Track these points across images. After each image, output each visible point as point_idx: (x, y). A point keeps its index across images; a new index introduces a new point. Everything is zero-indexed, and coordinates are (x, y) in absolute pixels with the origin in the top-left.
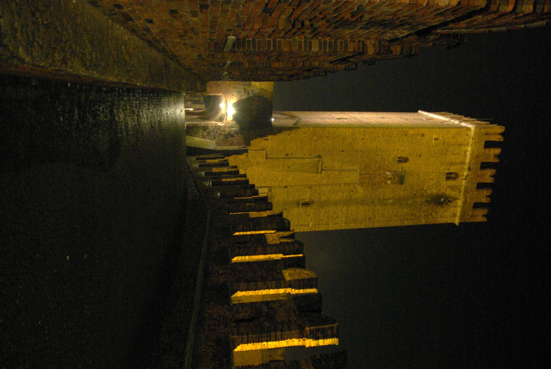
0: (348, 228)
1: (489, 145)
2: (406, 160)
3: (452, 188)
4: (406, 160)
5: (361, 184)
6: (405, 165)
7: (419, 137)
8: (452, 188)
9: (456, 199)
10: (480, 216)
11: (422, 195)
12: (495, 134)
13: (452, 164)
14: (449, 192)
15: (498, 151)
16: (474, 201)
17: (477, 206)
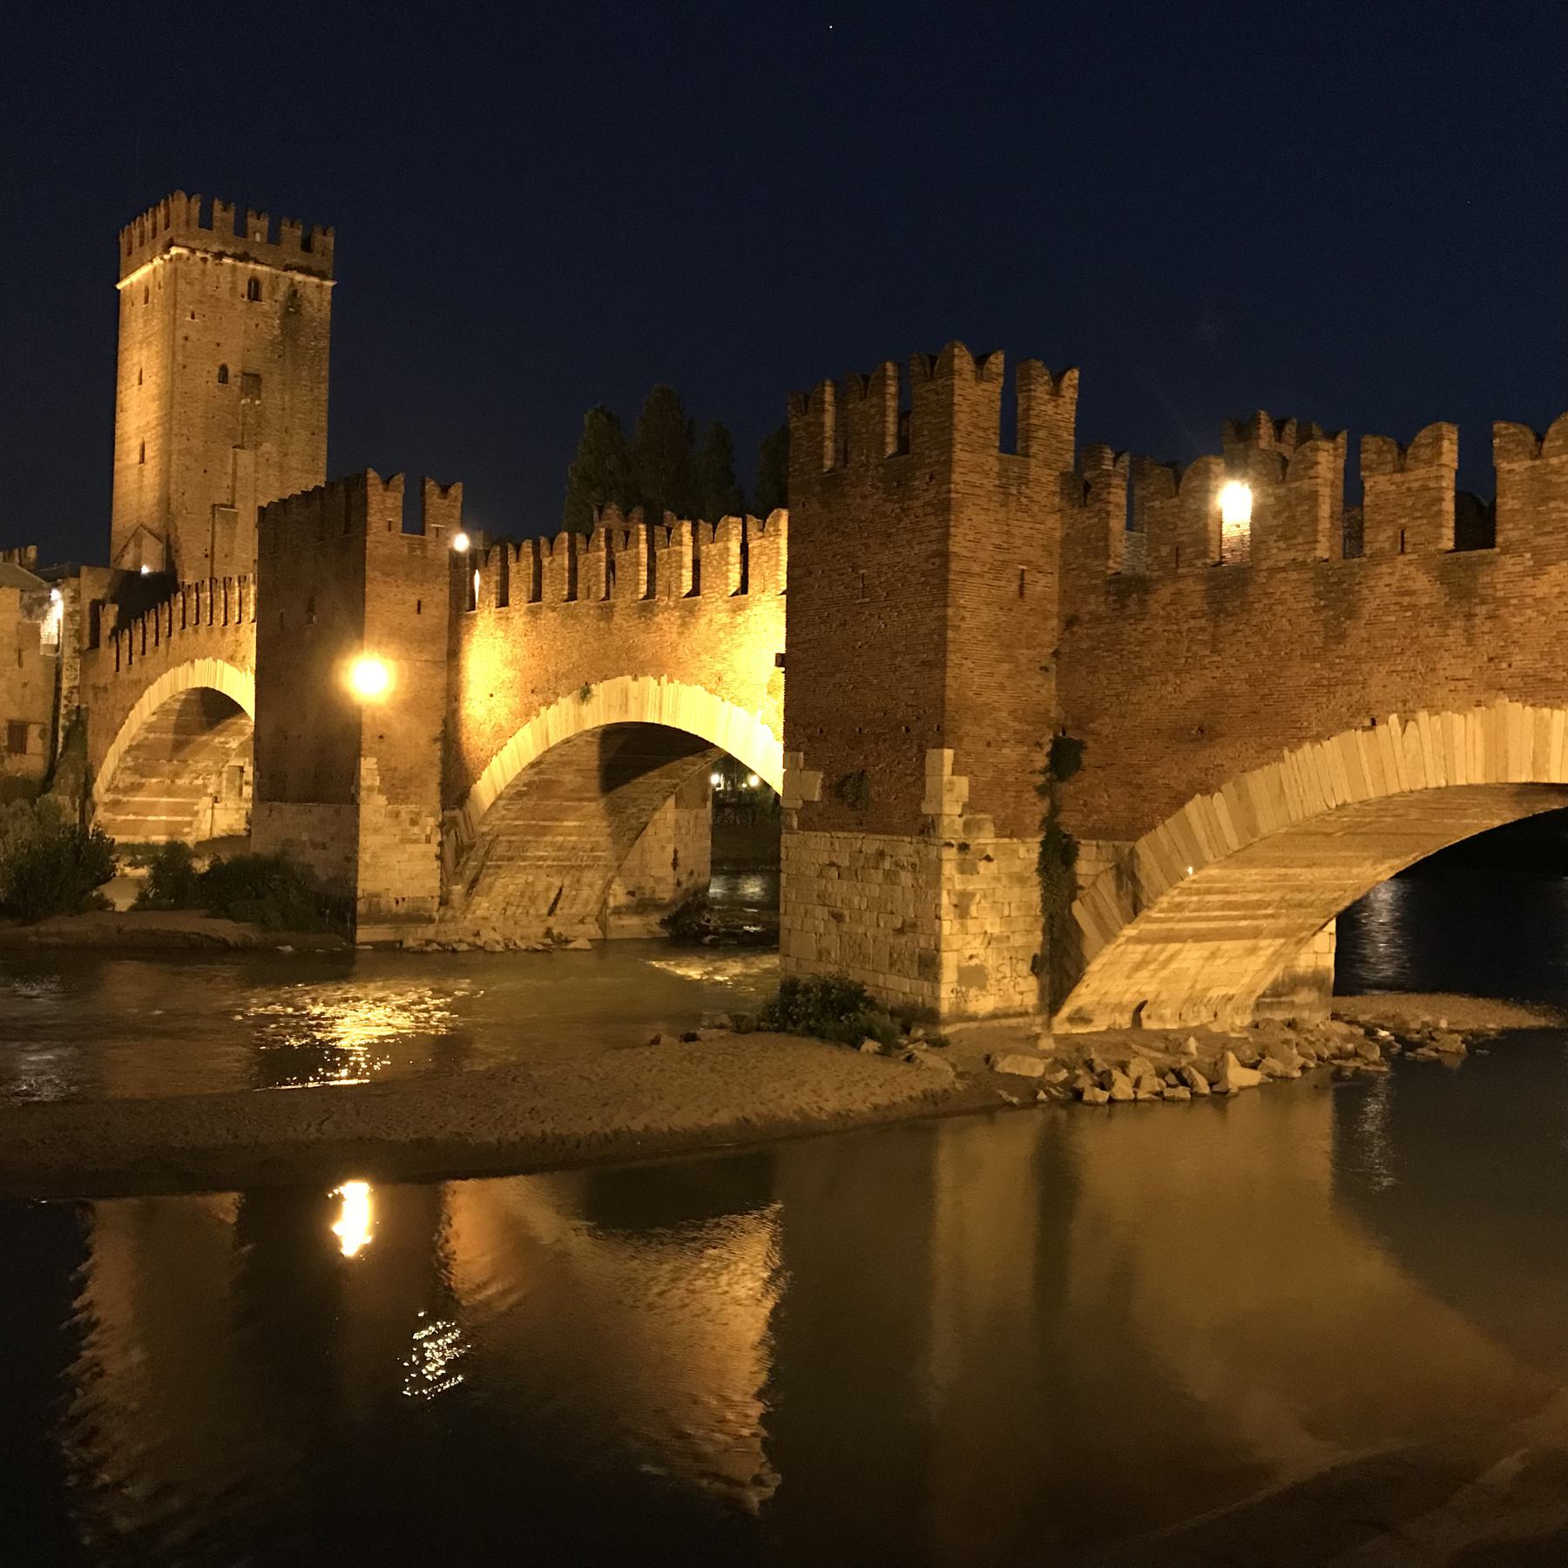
0: (324, 470)
1: (206, 222)
2: (224, 369)
3: (274, 290)
4: (224, 369)
5: (258, 445)
6: (231, 372)
7: (189, 344)
8: (274, 290)
9: (292, 284)
10: (326, 241)
11: (282, 343)
12: (188, 209)
13: (233, 290)
14: (280, 297)
15: (218, 205)
16: (299, 249)
17: (307, 245)
